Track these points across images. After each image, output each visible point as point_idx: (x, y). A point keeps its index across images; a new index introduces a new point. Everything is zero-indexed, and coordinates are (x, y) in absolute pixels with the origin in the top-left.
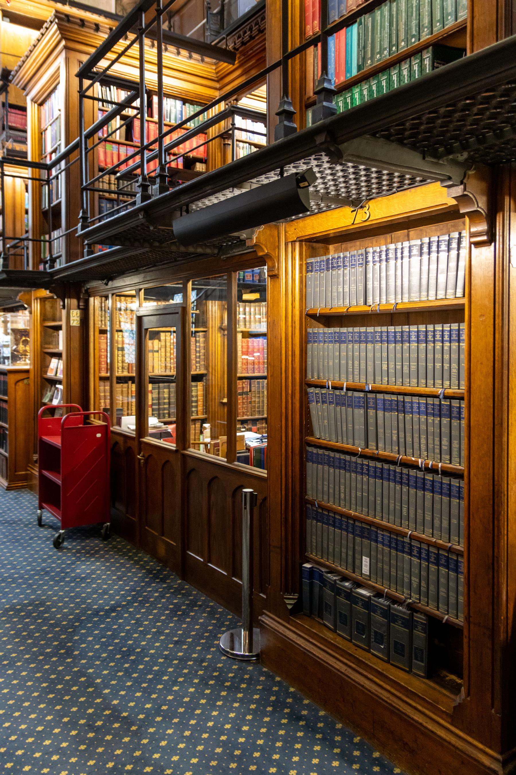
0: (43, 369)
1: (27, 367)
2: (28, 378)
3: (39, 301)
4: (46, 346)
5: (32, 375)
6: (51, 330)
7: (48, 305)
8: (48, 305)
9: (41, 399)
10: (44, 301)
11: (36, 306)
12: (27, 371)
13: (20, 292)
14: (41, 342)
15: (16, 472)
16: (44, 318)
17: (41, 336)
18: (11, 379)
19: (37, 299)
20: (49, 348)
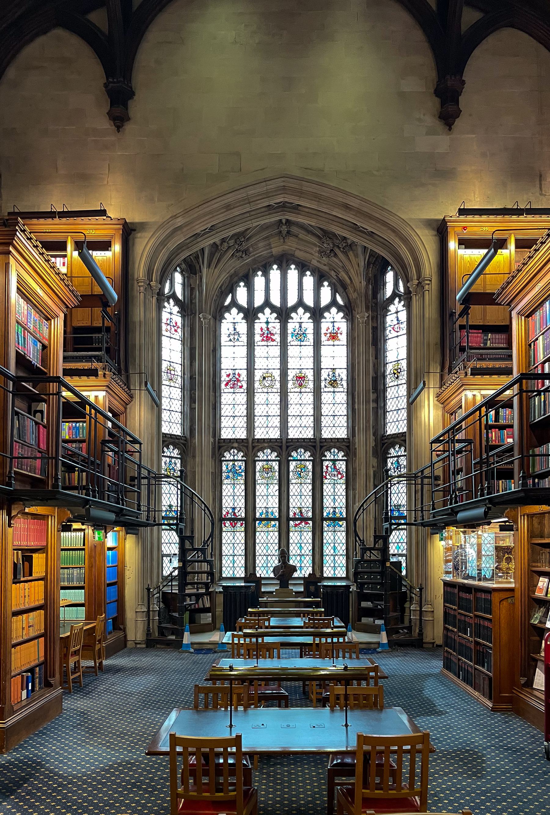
0: (531, 589)
1: (513, 585)
2: (513, 597)
3: (526, 517)
4: (534, 564)
5: (518, 594)
6: (539, 548)
7: (535, 521)
8: (535, 521)
9: (529, 620)
10: (532, 517)
11: (523, 524)
12: (511, 590)
13: (507, 509)
14: (529, 560)
15: (500, 693)
16: (532, 534)
17: (528, 554)
18: (496, 598)
19: (524, 516)
20: (537, 567)
